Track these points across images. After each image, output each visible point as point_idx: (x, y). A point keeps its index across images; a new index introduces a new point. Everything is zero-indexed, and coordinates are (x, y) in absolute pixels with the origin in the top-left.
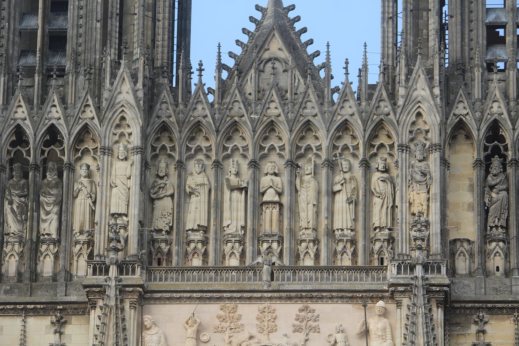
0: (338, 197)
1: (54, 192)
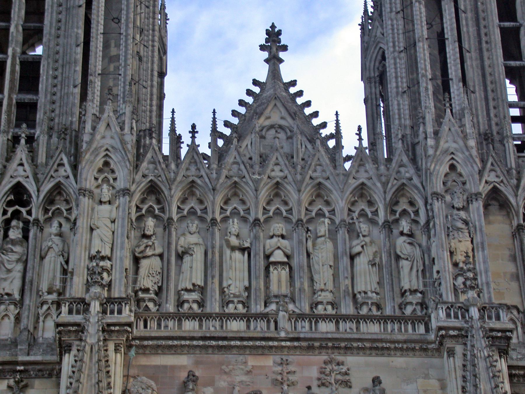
0: (357, 260)
1: (18, 249)
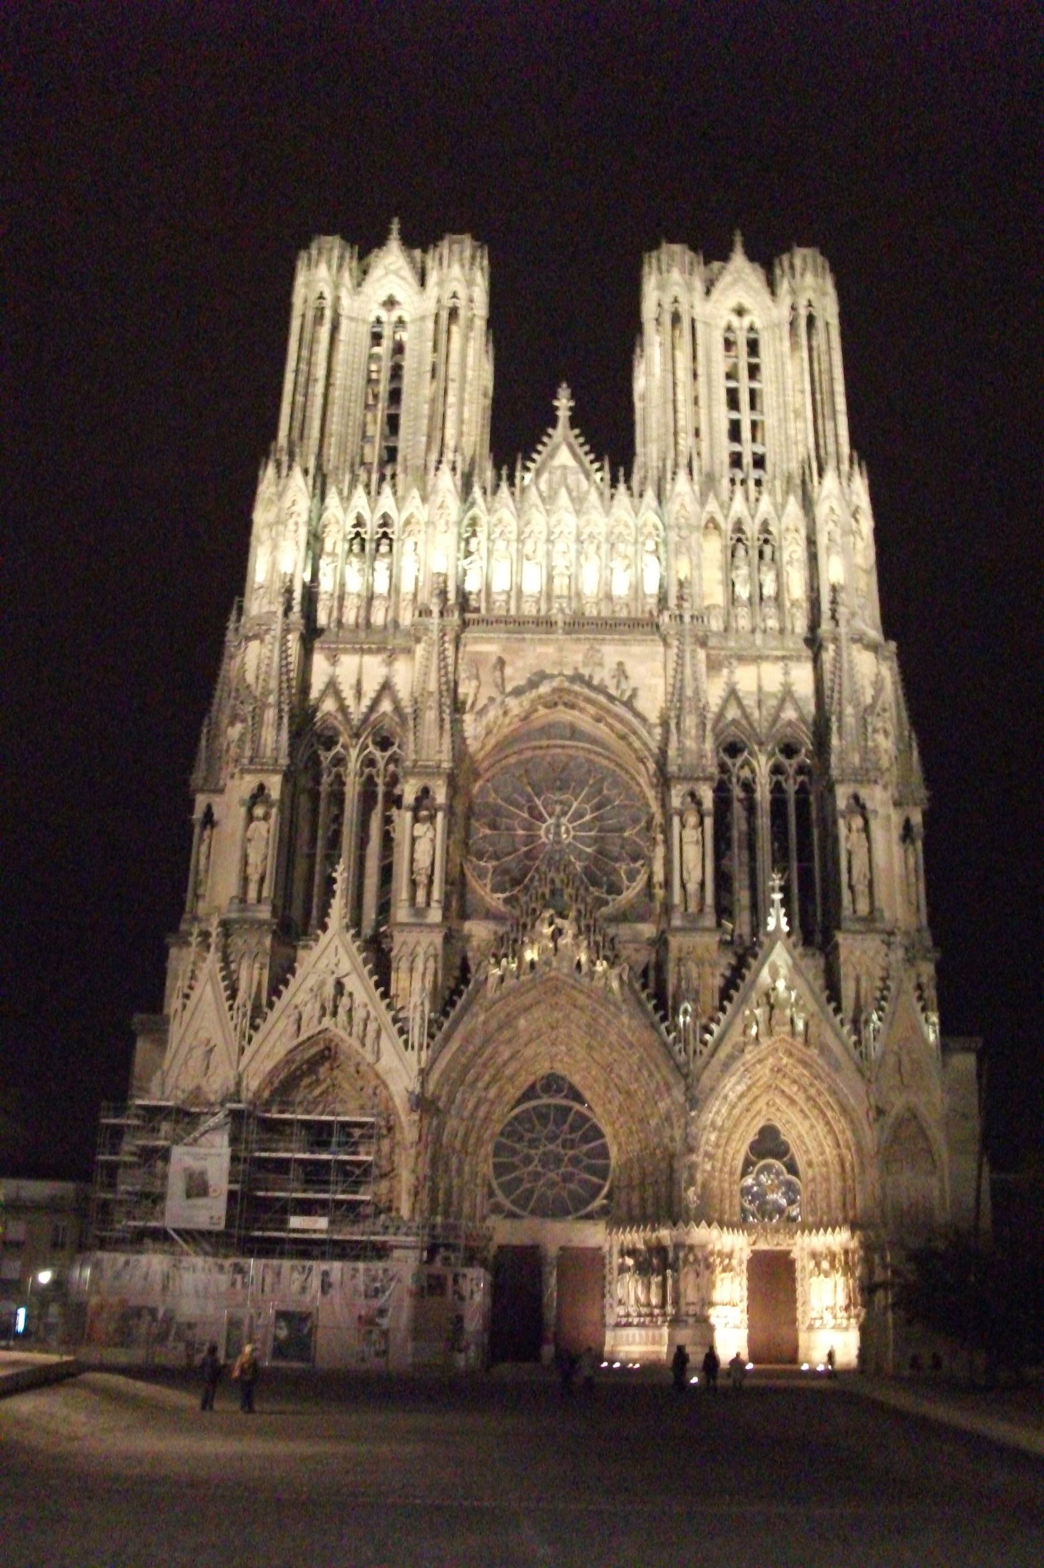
1: (387, 560)
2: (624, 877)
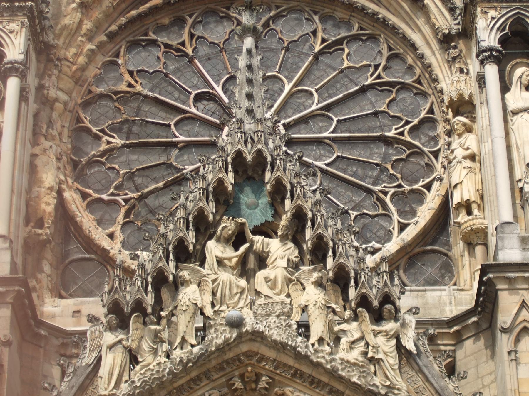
2: (393, 208)
